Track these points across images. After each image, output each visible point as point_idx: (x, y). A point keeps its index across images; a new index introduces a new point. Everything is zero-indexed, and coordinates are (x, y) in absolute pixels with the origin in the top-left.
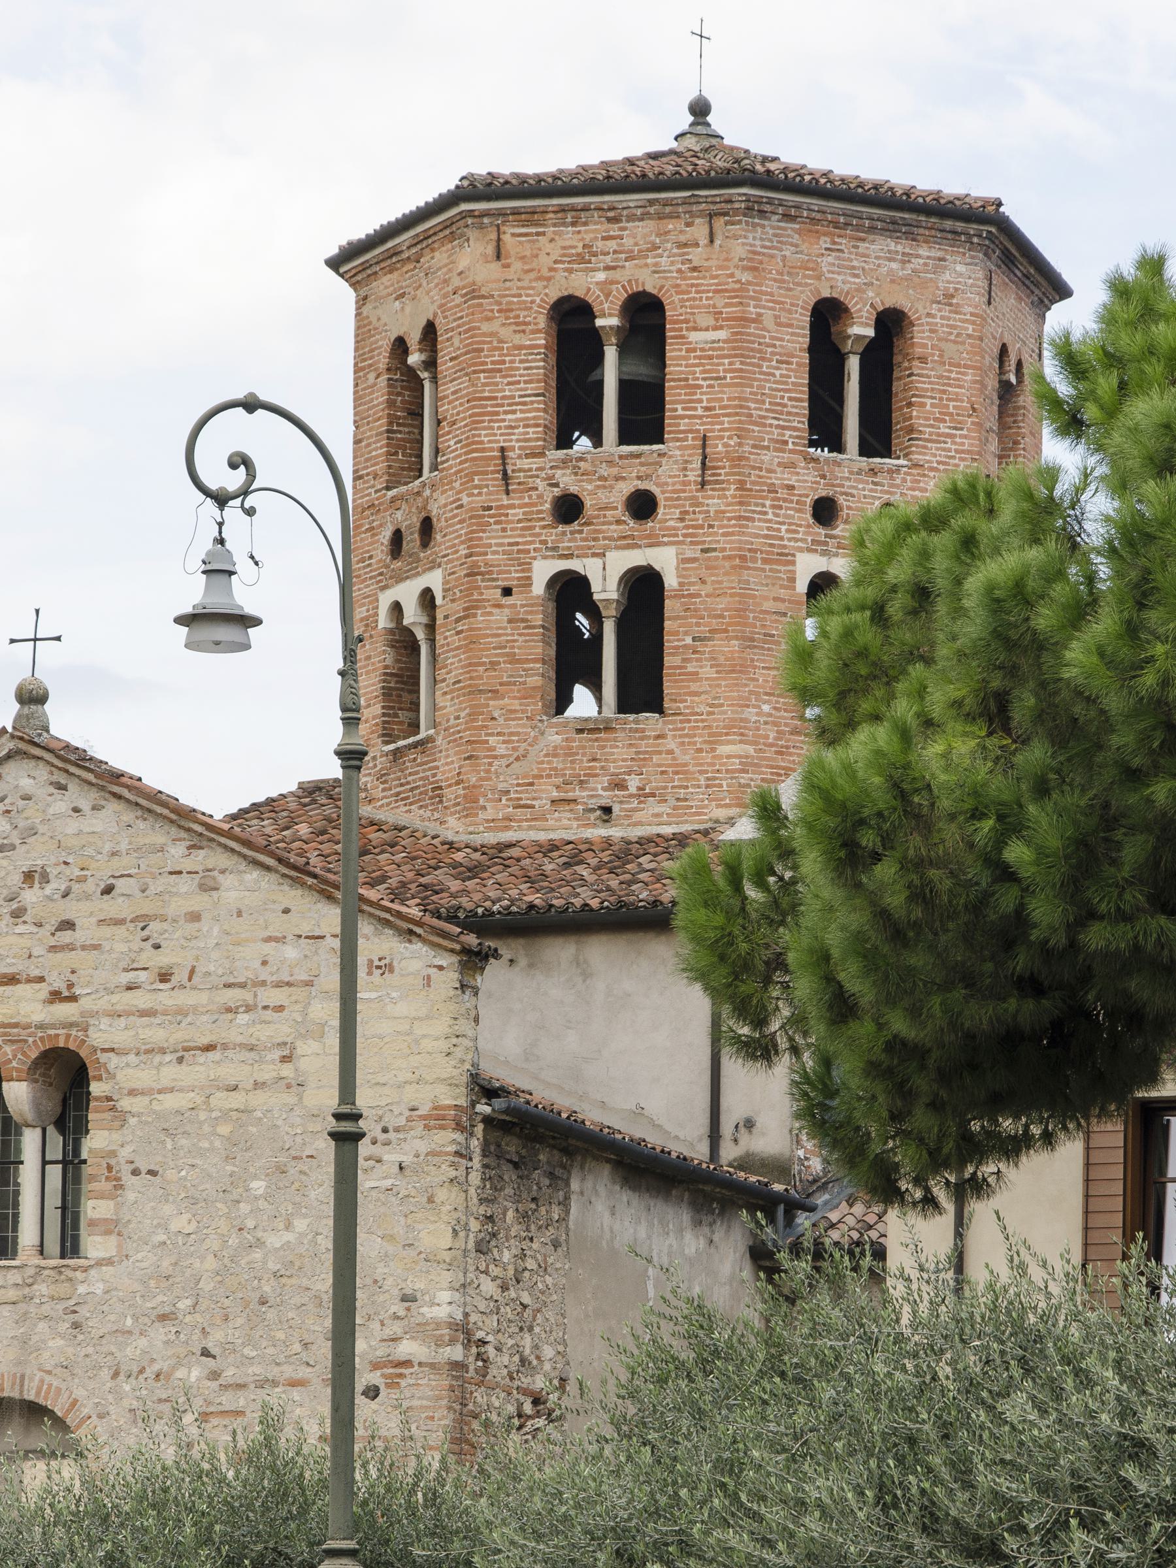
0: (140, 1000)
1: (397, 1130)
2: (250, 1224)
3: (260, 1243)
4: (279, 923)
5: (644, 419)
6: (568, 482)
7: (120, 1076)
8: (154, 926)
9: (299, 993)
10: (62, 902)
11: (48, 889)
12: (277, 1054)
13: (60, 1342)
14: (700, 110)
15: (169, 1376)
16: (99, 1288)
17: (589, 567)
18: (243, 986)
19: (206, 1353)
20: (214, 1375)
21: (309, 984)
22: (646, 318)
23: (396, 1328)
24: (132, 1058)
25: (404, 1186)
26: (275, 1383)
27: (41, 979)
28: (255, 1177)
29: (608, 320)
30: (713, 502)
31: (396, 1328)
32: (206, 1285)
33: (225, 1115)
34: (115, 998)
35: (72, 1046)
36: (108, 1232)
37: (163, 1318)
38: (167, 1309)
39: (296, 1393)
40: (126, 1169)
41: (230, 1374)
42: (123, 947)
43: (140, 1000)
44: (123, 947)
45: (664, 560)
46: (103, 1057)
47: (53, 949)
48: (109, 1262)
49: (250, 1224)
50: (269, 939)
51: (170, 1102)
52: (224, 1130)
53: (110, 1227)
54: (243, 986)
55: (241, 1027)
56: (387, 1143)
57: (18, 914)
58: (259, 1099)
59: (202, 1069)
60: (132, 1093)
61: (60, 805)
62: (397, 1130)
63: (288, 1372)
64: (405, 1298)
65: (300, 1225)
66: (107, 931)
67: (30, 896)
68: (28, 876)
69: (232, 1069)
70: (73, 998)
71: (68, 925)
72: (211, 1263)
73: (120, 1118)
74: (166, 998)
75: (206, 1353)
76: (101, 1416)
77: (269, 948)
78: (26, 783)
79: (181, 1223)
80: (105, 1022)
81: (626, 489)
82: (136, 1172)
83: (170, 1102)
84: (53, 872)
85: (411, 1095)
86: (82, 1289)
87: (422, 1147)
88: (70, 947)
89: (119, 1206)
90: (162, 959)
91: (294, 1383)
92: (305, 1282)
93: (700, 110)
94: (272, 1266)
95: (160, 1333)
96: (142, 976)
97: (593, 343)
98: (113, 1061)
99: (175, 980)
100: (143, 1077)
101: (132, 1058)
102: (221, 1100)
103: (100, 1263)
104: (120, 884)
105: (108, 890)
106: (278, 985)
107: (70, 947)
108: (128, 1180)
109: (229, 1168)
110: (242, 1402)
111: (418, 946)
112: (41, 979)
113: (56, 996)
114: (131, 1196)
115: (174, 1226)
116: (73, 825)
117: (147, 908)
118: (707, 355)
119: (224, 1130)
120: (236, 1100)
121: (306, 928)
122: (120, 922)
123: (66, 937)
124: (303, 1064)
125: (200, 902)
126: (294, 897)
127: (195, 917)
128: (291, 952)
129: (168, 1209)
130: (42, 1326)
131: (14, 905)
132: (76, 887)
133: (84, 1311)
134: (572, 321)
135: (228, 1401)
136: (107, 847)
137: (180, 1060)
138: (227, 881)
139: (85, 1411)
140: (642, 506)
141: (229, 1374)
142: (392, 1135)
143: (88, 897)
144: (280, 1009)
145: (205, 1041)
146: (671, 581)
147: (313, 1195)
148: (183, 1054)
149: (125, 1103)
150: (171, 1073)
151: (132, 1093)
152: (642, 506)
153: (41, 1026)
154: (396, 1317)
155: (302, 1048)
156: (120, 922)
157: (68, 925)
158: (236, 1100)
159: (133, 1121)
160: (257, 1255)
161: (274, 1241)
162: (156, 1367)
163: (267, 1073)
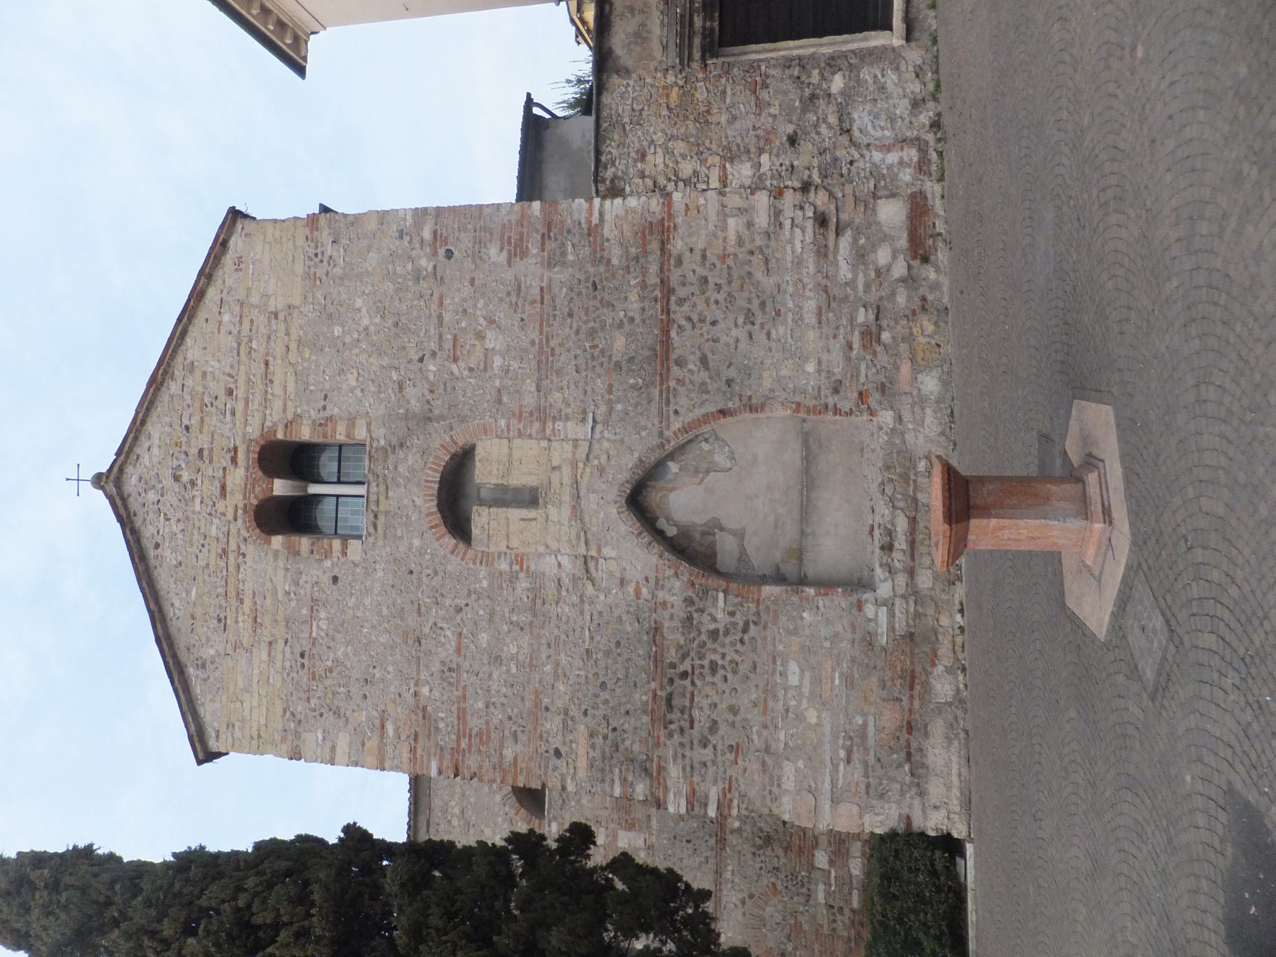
1: (316, 247)
2: (355, 336)
3: (366, 329)
4: (213, 326)
7: (275, 419)
8: (207, 400)
9: (246, 310)
10: (190, 457)
11: (183, 465)
12: (273, 321)
13: (410, 458)
15: (432, 384)
16: (382, 431)
18: (239, 345)
19: (421, 360)
20: (434, 354)
21: (242, 304)
23: (416, 240)
24: (268, 412)
25: (344, 241)
26: (440, 317)
27: (225, 469)
28: (332, 333)
31: (416, 240)
32: (385, 361)
33: (300, 353)
34: (238, 424)
35: (258, 449)
36: (354, 425)
37: (401, 388)
38: (396, 386)
39: (447, 301)
40: (323, 414)
41: (433, 346)
42: (214, 418)
43: (240, 407)
44: (214, 418)
46: (266, 430)
47: (211, 461)
48: (369, 424)
49: (355, 336)
50: (219, 330)
51: (291, 387)
52: (307, 354)
53: (351, 422)
54: (239, 345)
56: (323, 253)
57: (193, 483)
58: (294, 332)
59: (277, 368)
60: (284, 411)
61: (145, 459)
62: (316, 247)
63: (434, 307)
64: (401, 237)
65: (359, 303)
66: (206, 428)
68: (177, 478)
70: (236, 449)
71: (201, 451)
72: (372, 360)
73: (297, 417)
74: (240, 393)
75: (421, 360)
76: (452, 429)
77: (223, 330)
78: (134, 480)
79: (352, 379)
80: (249, 429)
82: (324, 408)
83: (291, 387)
84: (176, 463)
85: (300, 241)
86: (382, 443)
87: (326, 232)
88: (211, 450)
89: (341, 418)
90: (222, 393)
91: (441, 304)
92: (388, 299)
94: (378, 320)
95: (409, 391)
96: (229, 406)
98: (268, 423)
99: (232, 386)
100: (278, 404)
101: (268, 412)
102: (293, 357)
103: (369, 431)
104: (185, 422)
105: (187, 428)
106: (241, 323)
107: (211, 450)
108: (328, 413)
109: (327, 349)
110: (449, 337)
111: (232, 243)
112: (225, 469)
113: (234, 460)
114: (336, 410)
115: (354, 383)
116: (155, 450)
117: (197, 404)
119: (307, 354)
120: (293, 346)
121: (216, 309)
122: (202, 421)
123: (206, 453)
124: (280, 307)
125: (198, 374)
126: (201, 315)
127: (204, 374)
128: (226, 318)
129: (345, 387)
130: (400, 469)
131: (189, 486)
132: (184, 448)
133: (394, 441)
135: (448, 345)
136: (167, 429)
137: (271, 382)
138: (190, 356)
139: (448, 439)
141: (433, 346)
142: (319, 251)
143: (188, 442)
144: (252, 321)
145: (263, 366)
147: (344, 296)
149: (290, 416)
150: (277, 389)
151: (284, 411)
153: (247, 469)
154: (410, 242)
155: (272, 309)
156: (202, 421)
157: (201, 451)
158: (293, 346)
159: (299, 411)
160: (372, 329)
161: (365, 322)
162: (427, 393)
163: (282, 327)
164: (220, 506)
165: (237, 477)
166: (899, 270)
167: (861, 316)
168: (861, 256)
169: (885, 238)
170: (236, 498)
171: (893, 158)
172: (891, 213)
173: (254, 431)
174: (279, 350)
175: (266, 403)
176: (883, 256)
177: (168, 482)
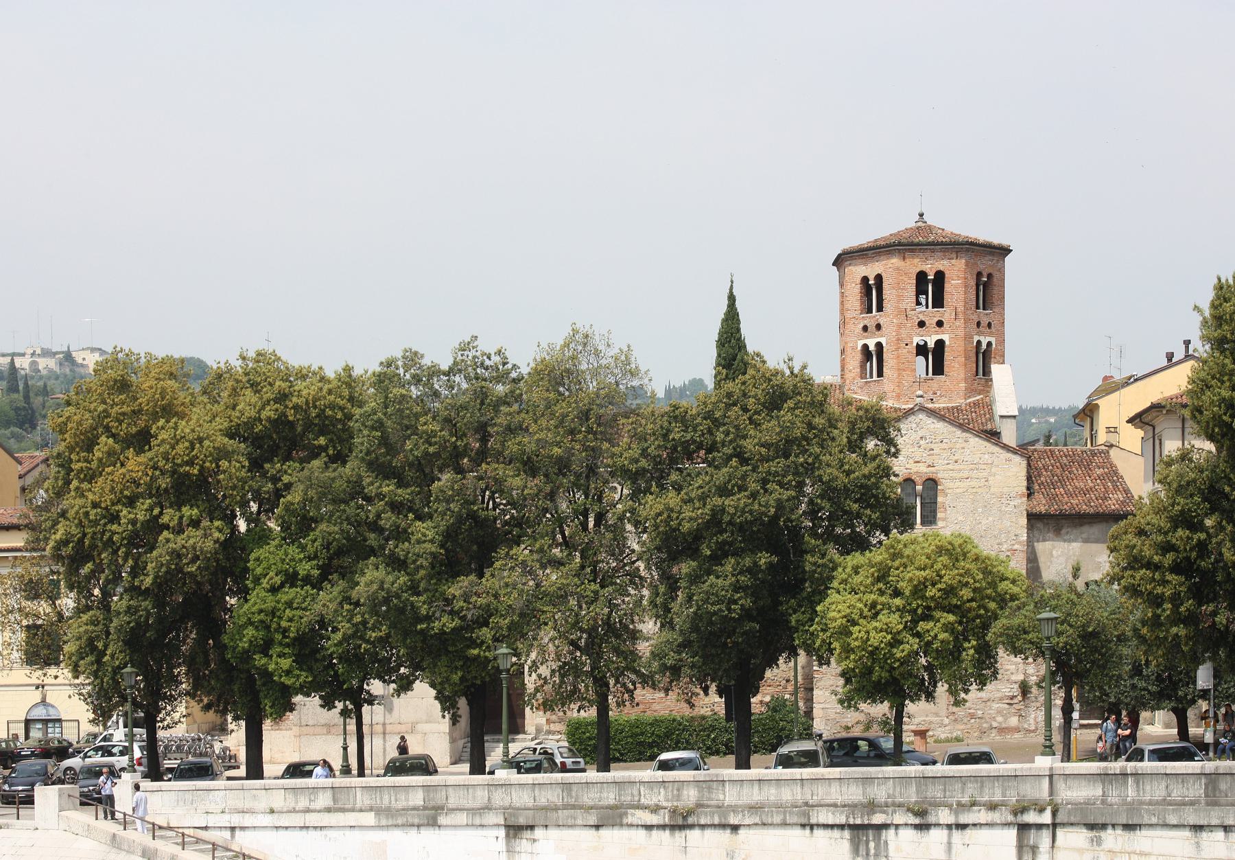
0: (950, 467)
4: (984, 450)
5: (938, 302)
6: (922, 318)
14: (921, 215)
17: (928, 339)
22: (940, 276)
29: (931, 277)
30: (958, 323)
43: (950, 467)
45: (946, 338)
53: (944, 519)
55: (974, 474)
67: (922, 442)
69: (974, 483)
74: (957, 466)
81: (936, 320)
93: (921, 215)
97: (927, 281)
100: (951, 485)
118: (956, 287)
125: (964, 445)
134: (921, 277)
140: (940, 324)
146: (947, 343)
148: (961, 479)
150: (958, 484)
152: (940, 324)
164: (911, 461)
165: (922, 468)
166: (995, 724)
167: (980, 712)
168: (999, 712)
169: (1006, 720)
170: (915, 468)
171: (1032, 721)
172: (1014, 721)
173: (940, 476)
174: (974, 483)
175: (952, 479)
176: (1000, 719)
177: (920, 433)
